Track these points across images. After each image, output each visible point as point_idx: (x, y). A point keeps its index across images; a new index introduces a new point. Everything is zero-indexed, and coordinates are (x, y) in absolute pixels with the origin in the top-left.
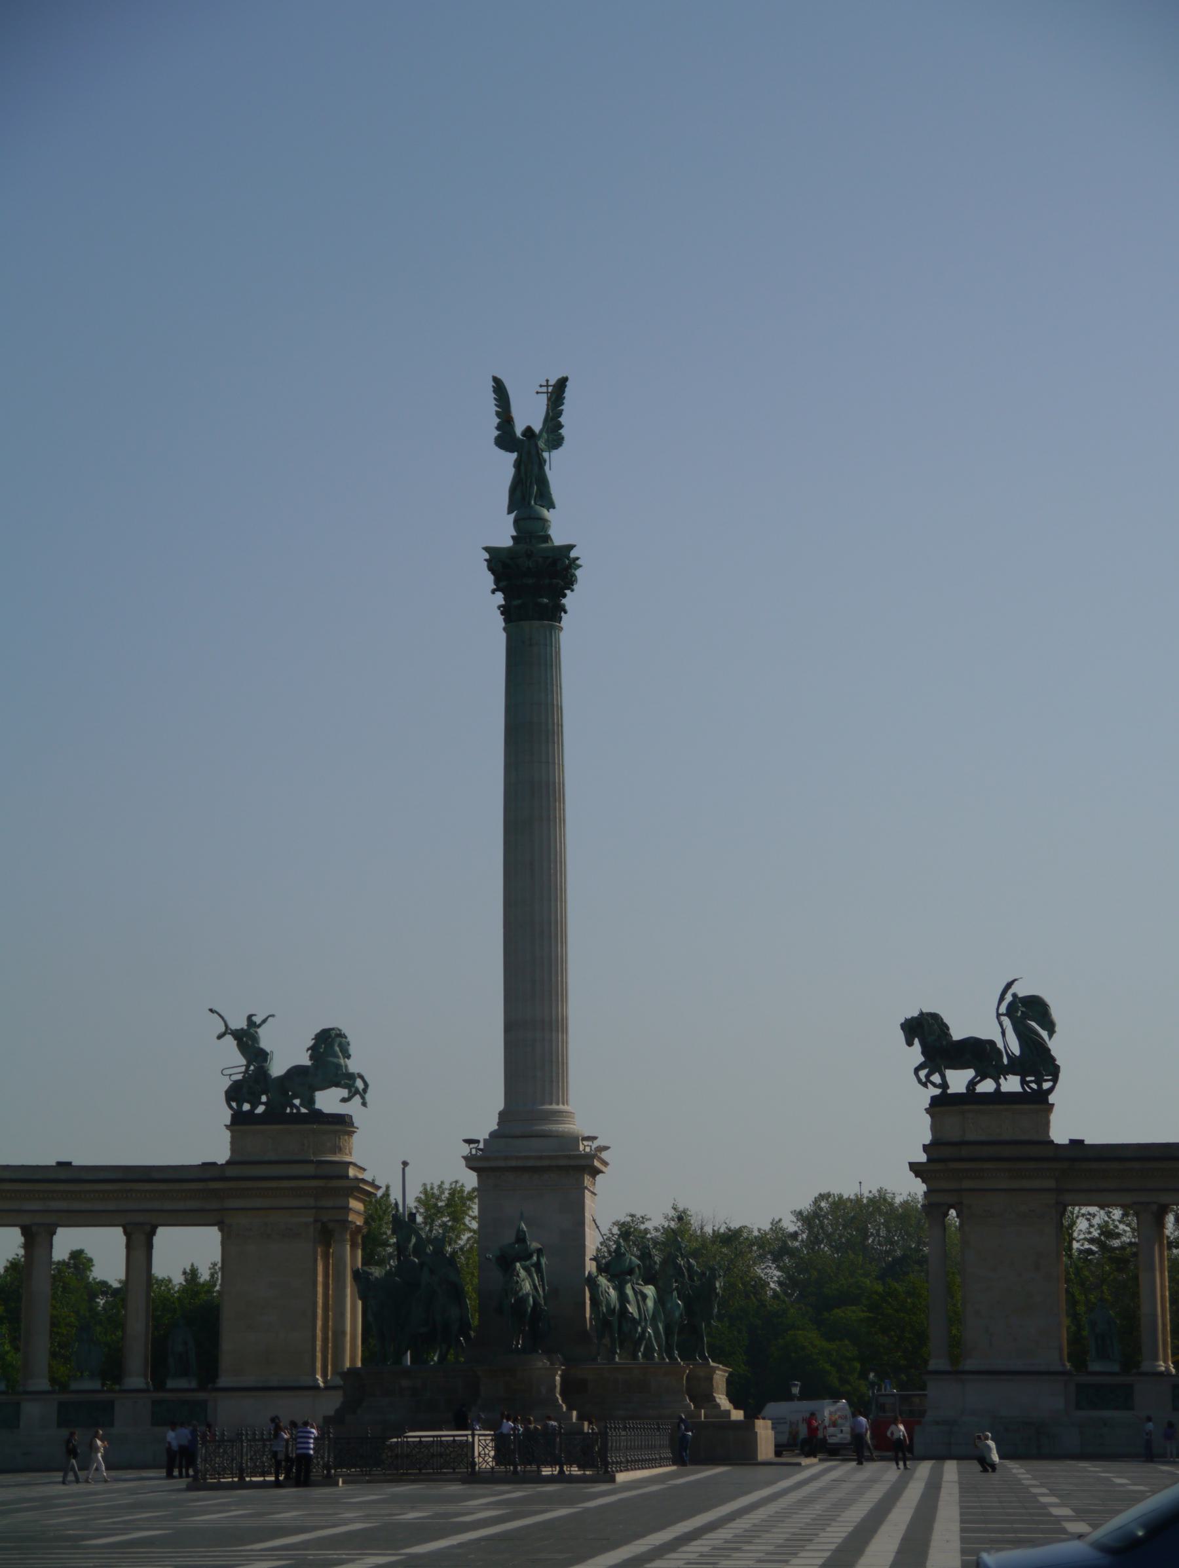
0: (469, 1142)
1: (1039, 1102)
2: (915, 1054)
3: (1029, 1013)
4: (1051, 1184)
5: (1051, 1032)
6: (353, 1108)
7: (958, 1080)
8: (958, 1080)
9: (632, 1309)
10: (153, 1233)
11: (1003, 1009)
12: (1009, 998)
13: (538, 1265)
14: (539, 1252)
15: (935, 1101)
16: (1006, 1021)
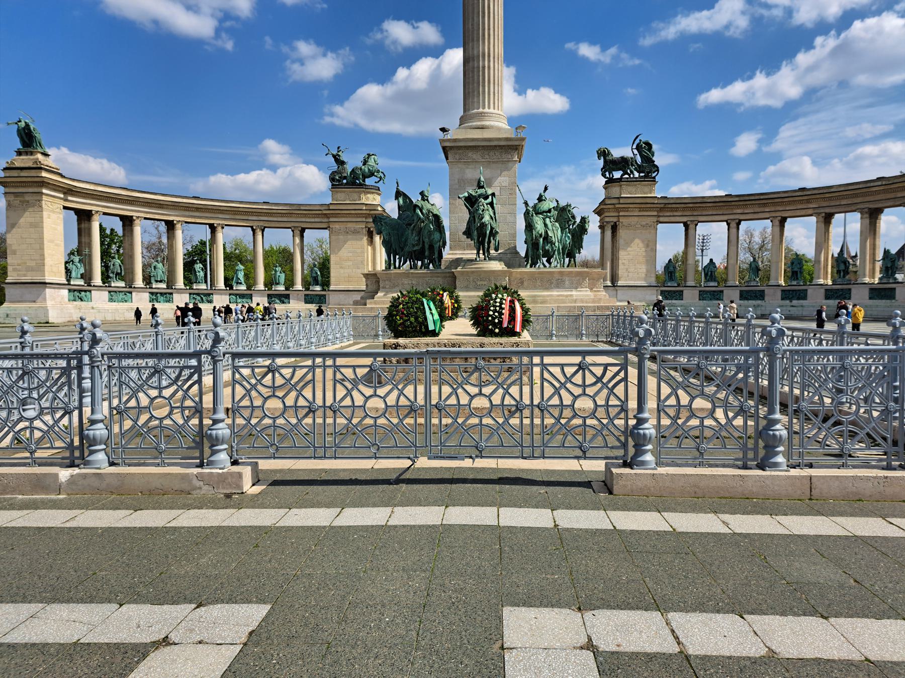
0: (443, 130)
1: (654, 180)
2: (602, 162)
3: (645, 149)
4: (655, 213)
5: (653, 155)
6: (380, 185)
7: (617, 175)
8: (617, 175)
9: (550, 234)
10: (303, 231)
11: (634, 147)
12: (637, 141)
13: (491, 204)
14: (493, 195)
15: (607, 183)
16: (636, 152)
